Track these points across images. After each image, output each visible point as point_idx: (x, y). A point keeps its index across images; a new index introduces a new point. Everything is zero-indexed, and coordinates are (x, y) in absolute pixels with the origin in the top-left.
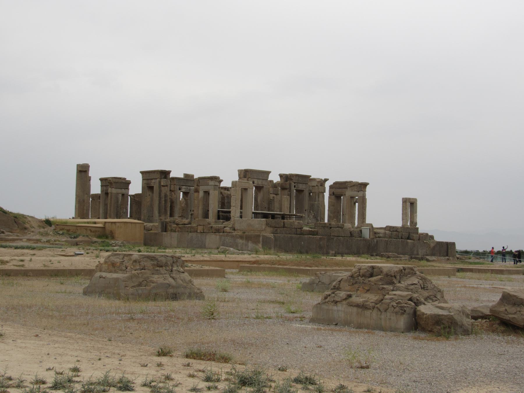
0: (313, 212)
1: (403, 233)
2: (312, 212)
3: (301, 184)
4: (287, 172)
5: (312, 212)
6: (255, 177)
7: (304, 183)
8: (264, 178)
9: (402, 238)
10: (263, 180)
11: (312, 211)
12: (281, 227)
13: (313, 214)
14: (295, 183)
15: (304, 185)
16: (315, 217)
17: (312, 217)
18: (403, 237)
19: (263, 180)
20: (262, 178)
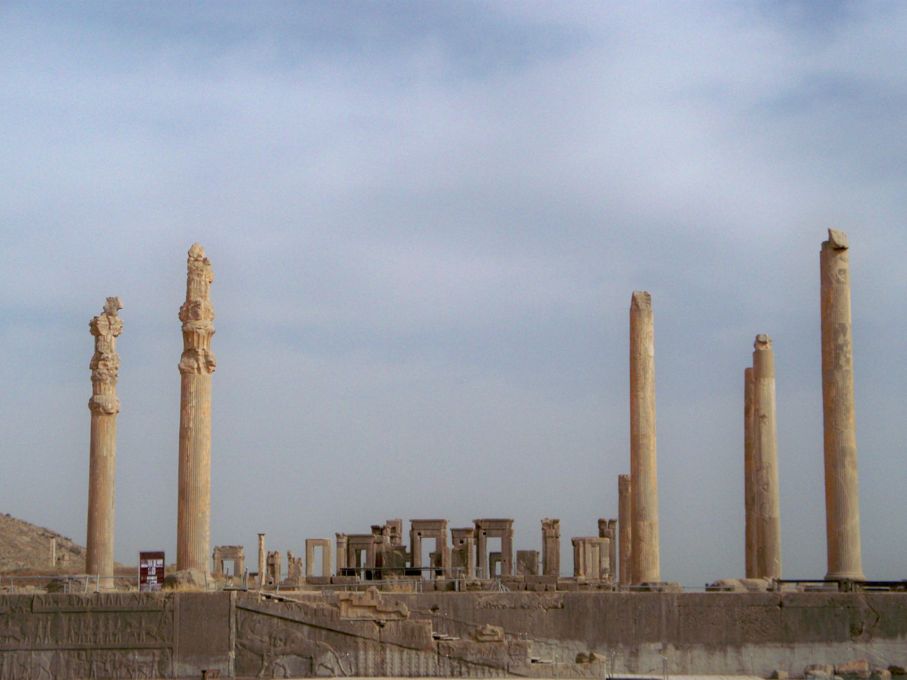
0: (525, 561)
1: (528, 584)
2: (522, 562)
3: (494, 531)
4: (480, 517)
5: (522, 562)
6: (421, 528)
7: (499, 529)
8: (435, 528)
9: (526, 589)
10: (434, 530)
11: (523, 561)
12: (327, 584)
13: (525, 565)
14: (485, 530)
15: (501, 531)
16: (528, 569)
17: (523, 568)
18: (528, 588)
19: (434, 530)
20: (432, 528)
